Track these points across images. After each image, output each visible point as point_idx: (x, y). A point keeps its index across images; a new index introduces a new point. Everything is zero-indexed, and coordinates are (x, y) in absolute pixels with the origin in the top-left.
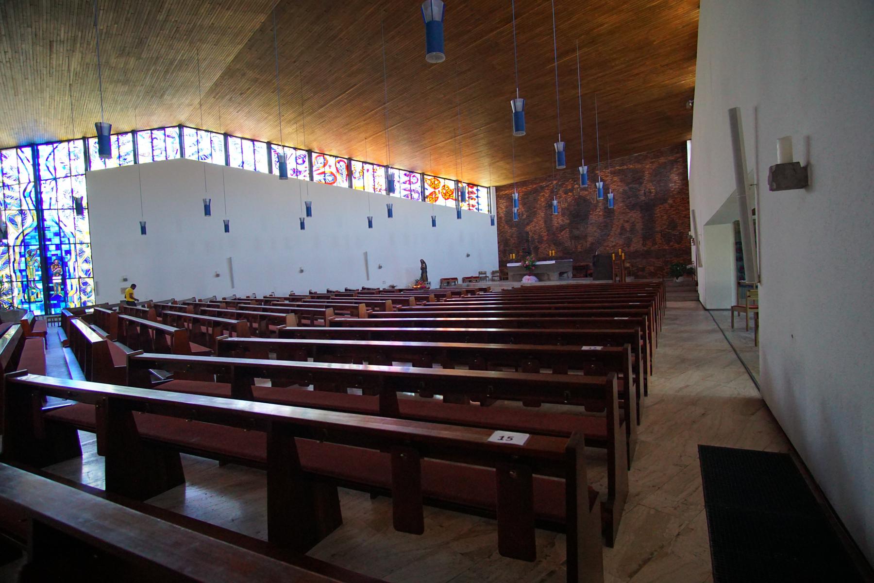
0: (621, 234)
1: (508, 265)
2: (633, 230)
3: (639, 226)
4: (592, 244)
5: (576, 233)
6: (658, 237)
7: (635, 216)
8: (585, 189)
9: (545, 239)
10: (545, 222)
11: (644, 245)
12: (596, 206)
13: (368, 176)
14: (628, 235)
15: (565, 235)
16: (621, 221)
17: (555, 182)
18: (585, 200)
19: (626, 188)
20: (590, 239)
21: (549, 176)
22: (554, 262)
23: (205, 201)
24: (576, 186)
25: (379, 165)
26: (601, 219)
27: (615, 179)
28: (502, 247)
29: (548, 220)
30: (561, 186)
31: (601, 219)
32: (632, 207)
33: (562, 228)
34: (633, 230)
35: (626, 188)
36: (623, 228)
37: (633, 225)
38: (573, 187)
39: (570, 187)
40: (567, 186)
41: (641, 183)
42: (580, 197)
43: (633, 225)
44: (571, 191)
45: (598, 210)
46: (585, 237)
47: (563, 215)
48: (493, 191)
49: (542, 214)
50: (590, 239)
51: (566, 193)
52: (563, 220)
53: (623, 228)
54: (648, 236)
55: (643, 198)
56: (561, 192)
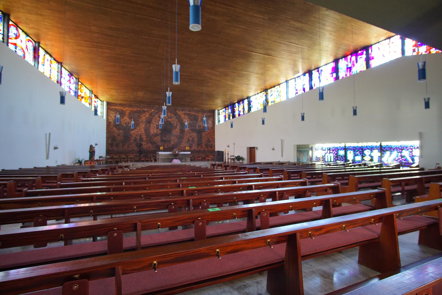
0: (187, 142)
2: (193, 141)
3: (196, 139)
4: (173, 145)
5: (165, 138)
6: (204, 144)
7: (195, 135)
8: (171, 118)
9: (145, 139)
10: (145, 131)
11: (198, 148)
12: (176, 127)
13: (47, 63)
14: (191, 142)
16: (188, 136)
17: (153, 110)
18: (170, 123)
19: (191, 122)
20: (172, 143)
21: (150, 106)
22: (190, 153)
23: (353, 107)
25: (55, 60)
26: (178, 134)
27: (186, 117)
28: (110, 141)
29: (147, 130)
30: (157, 113)
31: (178, 134)
32: (193, 131)
33: (156, 135)
34: (193, 141)
35: (191, 122)
36: (189, 139)
37: (193, 139)
41: (197, 121)
42: (167, 121)
43: (193, 139)
46: (169, 141)
48: (105, 103)
49: (144, 126)
50: (172, 143)
52: (157, 131)
53: (189, 139)
54: (199, 144)
55: (198, 128)
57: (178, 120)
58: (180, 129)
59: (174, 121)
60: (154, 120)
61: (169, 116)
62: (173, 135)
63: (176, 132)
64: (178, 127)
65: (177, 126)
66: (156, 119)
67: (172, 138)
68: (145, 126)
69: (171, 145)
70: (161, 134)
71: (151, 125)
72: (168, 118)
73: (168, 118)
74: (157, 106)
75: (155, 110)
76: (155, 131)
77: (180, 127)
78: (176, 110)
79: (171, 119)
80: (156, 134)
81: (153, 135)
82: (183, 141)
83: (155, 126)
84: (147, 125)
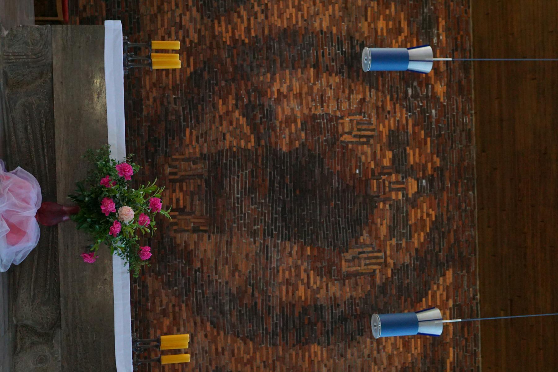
1: (113, 29)
5: (236, 183)
10: (289, 35)
12: (328, 271)
15: (228, 129)
18: (358, 223)
20: (206, 247)
24: (412, 186)
26: (279, 293)
30: (423, 119)
31: (279, 293)
33: (259, 115)
38: (410, 172)
39: (413, 157)
40: (421, 145)
42: (370, 203)
44: (399, 164)
45: (315, 281)
46: (215, 223)
47: (312, 123)
49: (322, 23)
50: (206, 247)
51: (396, 140)
52: (289, 120)
56: (401, 115)
57: (383, 289)
58: (319, 309)
59: (378, 252)
60: (371, 96)
61: (414, 216)
62: (265, 249)
63: (295, 274)
64: (334, 289)
65: (343, 278)
66: (380, 110)
67: (245, 246)
68: (325, 37)
69: (181, 238)
70: (273, 153)
71: (335, 80)
72: (397, 208)
73: (397, 208)
74: (470, 121)
75: (443, 110)
76: (291, 107)
77: (335, 302)
78: (462, 263)
79: (392, 230)
80: (269, 115)
81: (261, 93)
82: (224, 340)
83: (331, 108)
84: (330, 50)
